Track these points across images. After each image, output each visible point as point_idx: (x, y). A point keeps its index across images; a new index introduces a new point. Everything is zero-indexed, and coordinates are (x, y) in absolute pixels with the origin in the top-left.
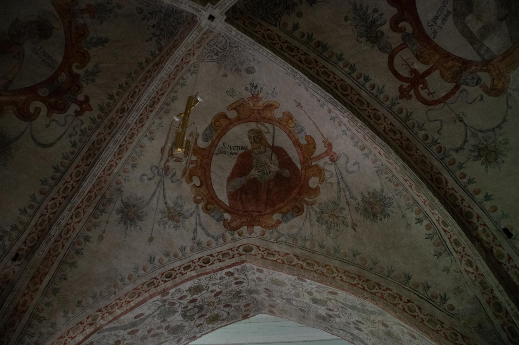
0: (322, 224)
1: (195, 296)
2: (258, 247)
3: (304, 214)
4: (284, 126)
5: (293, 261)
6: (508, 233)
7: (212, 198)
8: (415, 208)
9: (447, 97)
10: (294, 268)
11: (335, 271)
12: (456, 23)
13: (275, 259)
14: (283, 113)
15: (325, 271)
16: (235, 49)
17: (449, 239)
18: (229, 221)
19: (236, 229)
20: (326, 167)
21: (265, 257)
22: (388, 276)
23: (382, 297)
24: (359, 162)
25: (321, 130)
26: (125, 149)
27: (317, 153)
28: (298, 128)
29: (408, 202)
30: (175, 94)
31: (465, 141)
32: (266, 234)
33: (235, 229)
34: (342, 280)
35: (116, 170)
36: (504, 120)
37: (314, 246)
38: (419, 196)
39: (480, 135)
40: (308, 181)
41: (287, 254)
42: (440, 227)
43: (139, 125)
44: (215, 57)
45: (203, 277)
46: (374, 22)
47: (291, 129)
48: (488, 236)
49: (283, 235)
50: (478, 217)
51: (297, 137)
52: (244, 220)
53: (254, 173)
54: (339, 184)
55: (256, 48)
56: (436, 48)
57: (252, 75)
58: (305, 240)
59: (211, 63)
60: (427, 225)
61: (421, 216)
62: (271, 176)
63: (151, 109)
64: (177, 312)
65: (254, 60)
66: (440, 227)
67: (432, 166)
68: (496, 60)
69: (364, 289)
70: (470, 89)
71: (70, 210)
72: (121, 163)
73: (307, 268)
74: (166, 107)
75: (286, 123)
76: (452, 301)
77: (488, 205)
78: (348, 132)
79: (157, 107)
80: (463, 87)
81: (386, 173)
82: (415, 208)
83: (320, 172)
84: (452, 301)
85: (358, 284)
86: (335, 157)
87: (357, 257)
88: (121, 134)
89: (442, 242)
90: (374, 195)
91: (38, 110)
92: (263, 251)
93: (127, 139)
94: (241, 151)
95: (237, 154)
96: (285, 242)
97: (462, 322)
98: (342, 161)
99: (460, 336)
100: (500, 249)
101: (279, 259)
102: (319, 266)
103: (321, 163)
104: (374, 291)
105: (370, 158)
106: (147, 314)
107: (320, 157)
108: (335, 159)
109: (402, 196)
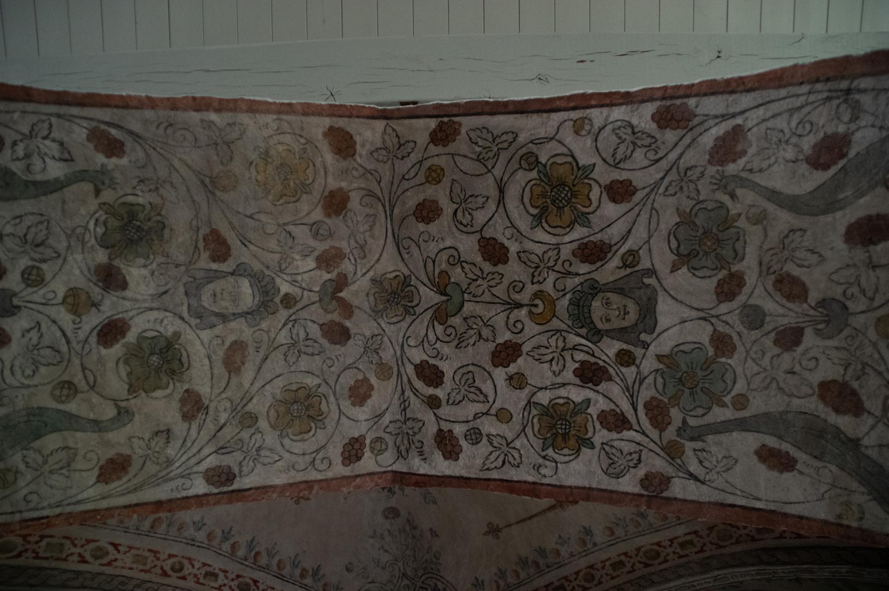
1: (577, 395)
16: (409, 573)
26: (641, 553)
30: (519, 570)
35: (680, 531)
43: (598, 575)
45: (525, 475)
57: (389, 506)
59: (448, 579)
63: (566, 584)
64: (659, 358)
65: (382, 535)
72: (663, 536)
74: (541, 562)
106: (751, 441)
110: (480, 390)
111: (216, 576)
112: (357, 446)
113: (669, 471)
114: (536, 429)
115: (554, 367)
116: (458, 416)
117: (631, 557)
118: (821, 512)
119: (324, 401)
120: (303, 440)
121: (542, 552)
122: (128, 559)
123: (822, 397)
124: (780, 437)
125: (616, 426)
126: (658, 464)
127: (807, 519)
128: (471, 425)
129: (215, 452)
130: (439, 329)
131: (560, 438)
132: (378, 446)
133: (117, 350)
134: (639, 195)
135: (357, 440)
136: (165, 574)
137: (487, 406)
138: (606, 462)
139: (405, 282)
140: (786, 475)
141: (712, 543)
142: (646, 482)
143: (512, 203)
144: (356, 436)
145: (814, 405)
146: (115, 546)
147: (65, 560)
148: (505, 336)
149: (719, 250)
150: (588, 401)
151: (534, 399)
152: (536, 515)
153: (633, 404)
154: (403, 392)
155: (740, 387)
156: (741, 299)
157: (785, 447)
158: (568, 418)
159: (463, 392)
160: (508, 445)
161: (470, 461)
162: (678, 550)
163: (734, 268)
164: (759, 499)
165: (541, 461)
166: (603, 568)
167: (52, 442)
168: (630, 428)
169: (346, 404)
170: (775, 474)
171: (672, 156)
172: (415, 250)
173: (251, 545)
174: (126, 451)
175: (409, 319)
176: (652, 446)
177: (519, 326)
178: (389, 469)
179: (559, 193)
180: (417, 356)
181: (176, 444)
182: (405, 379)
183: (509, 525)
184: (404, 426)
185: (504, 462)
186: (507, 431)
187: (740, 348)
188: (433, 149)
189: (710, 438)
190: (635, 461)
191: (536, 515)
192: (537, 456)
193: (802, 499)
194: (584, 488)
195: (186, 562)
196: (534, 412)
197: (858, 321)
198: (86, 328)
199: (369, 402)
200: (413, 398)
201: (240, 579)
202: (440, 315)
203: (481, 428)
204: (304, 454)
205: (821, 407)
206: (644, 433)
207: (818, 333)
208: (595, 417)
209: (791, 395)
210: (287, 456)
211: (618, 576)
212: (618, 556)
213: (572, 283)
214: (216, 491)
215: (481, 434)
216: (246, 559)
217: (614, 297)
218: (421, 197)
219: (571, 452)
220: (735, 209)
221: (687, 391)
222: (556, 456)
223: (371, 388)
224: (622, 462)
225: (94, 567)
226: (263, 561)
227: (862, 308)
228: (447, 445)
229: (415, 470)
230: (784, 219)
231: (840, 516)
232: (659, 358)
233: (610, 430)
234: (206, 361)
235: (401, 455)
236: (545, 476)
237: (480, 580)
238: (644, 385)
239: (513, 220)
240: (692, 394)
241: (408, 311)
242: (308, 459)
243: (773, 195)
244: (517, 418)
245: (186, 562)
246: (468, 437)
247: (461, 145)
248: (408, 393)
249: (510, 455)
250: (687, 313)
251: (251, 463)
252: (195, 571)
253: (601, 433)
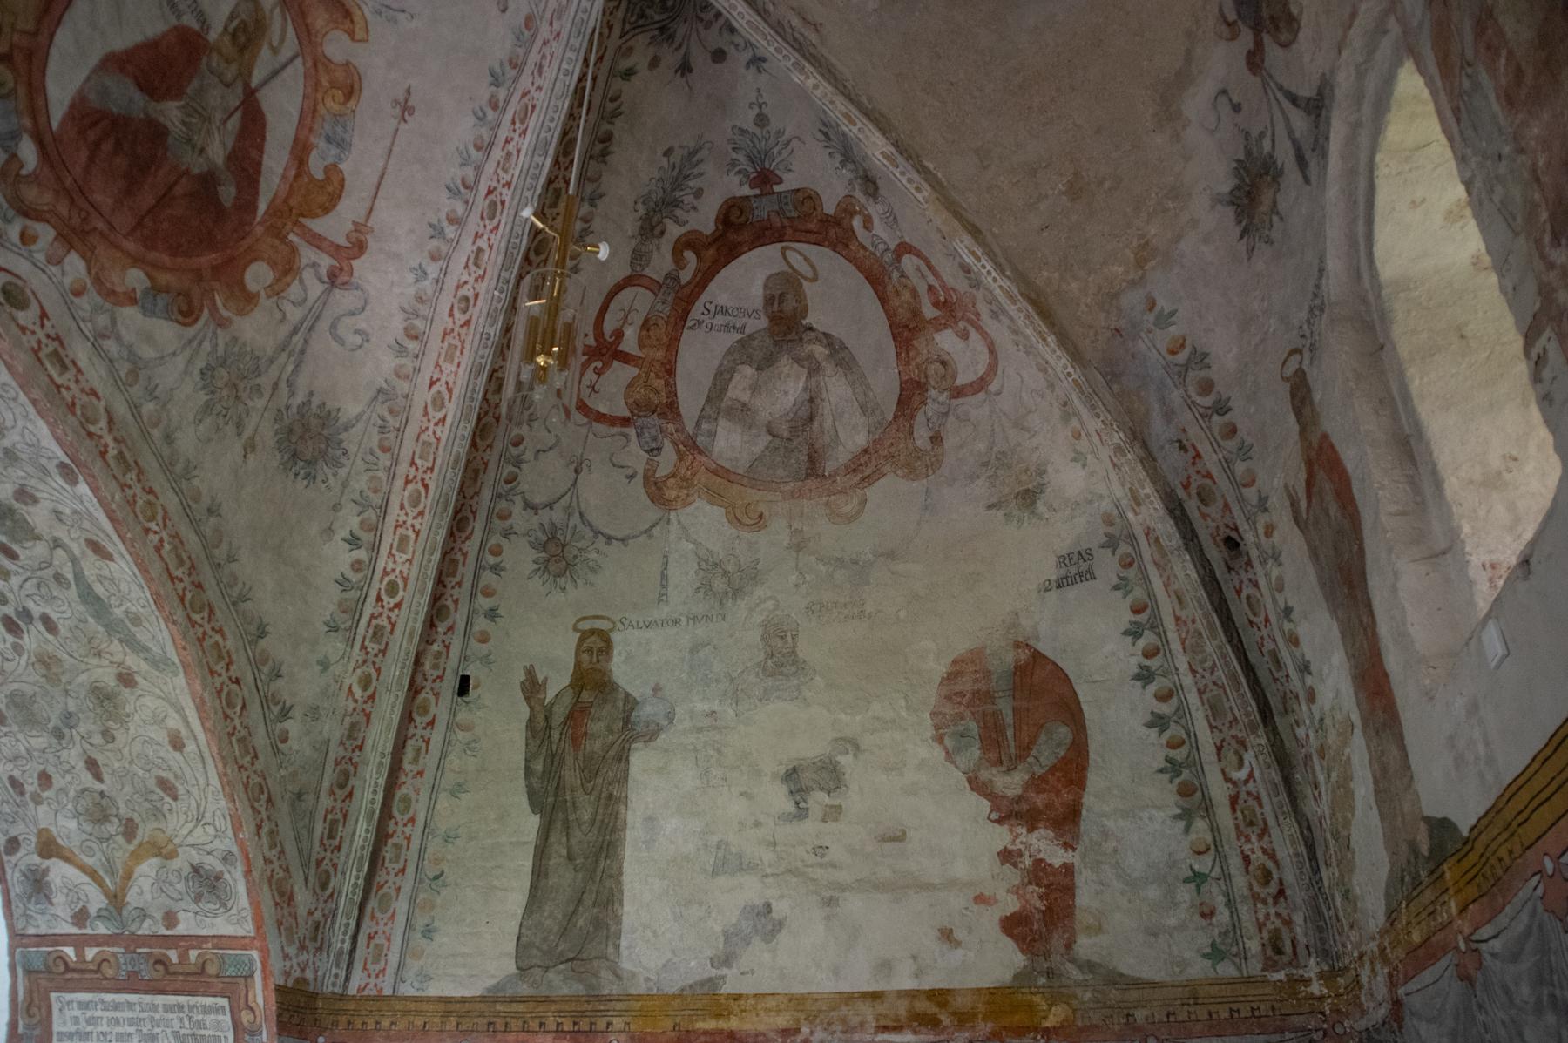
0: (204, 388)
2: (44, 315)
3: (191, 331)
4: (317, 84)
5: (94, 422)
6: (464, 686)
7: (30, 55)
8: (371, 515)
9: (601, 418)
10: (88, 441)
11: (159, 518)
12: (729, 352)
13: (59, 380)
14: (348, 64)
15: (140, 502)
17: (372, 617)
18: (24, 172)
19: (26, 214)
20: (308, 275)
21: (42, 355)
22: (234, 604)
23: (201, 640)
24: (373, 339)
25: (380, 203)
27: (318, 225)
28: (339, 129)
29: (372, 495)
31: (549, 506)
32: (85, 298)
33: (26, 212)
34: (158, 549)
36: (622, 540)
37: (156, 425)
38: (402, 507)
39: (575, 520)
40: (251, 262)
41: (94, 393)
42: (378, 585)
46: (676, 203)
47: (322, 110)
48: (436, 666)
49: (119, 339)
50: (451, 629)
51: (313, 139)
52: (63, 209)
53: (171, 113)
54: (295, 331)
55: (572, 41)
56: (673, 343)
58: (151, 393)
60: (359, 562)
61: (366, 537)
62: (198, 166)
66: (378, 585)
67: (477, 493)
68: (704, 459)
69: (182, 599)
70: (634, 445)
73: (112, 463)
75: (325, 84)
76: (293, 726)
77: (481, 624)
78: (427, 283)
80: (632, 432)
81: (391, 411)
82: (371, 515)
83: (287, 269)
84: (293, 726)
85: (181, 580)
86: (343, 278)
87: (212, 520)
89: (355, 611)
90: (327, 417)
92: (48, 336)
94: (189, 20)
95: (179, 17)
96: (111, 361)
97: (283, 772)
98: (344, 299)
99: (264, 797)
100: (433, 699)
101: (68, 388)
102: (139, 481)
103: (307, 254)
104: (196, 617)
105: (403, 361)
107: (317, 241)
108: (339, 281)
109: (371, 473)
111: (480, 250)
122: (449, 368)
133: (16, 548)
136: (467, 323)
146: (432, 383)
147: (438, 440)
167: (99, 589)
173: (453, 192)
174: (82, 541)
181: (60, 508)
195: (462, 292)
198: (14, 567)
210: (20, 423)
216: (467, 202)
225: (452, 409)
242: (12, 404)
245: (462, 292)
252: (472, 280)
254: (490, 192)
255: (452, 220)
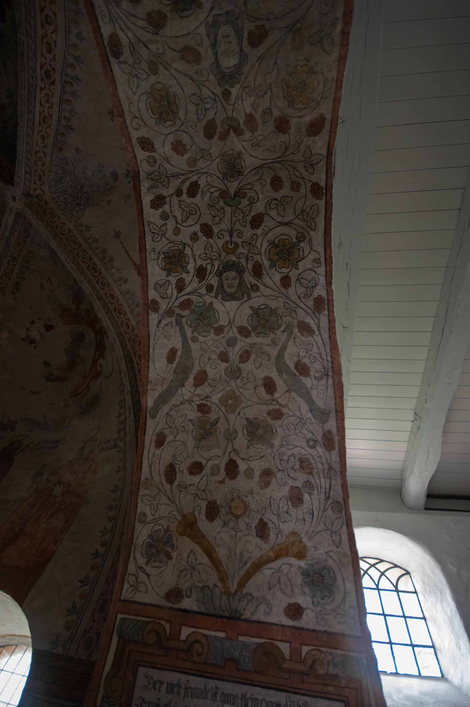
1: (191, 267)
26: (120, 307)
44: (82, 207)
45: (149, 244)
63: (98, 273)
64: (211, 303)
71: (125, 377)
79: (100, 265)
88: (94, 303)
91: (101, 366)
93: (112, 301)
106: (178, 345)
110: (188, 218)
112: (149, 147)
113: (161, 312)
114: (172, 248)
115: (203, 256)
116: (173, 206)
117: (117, 302)
118: (152, 375)
119: (172, 123)
120: (147, 110)
121: (111, 260)
123: (200, 372)
124: (181, 356)
125: (178, 286)
126: (163, 306)
127: (148, 370)
128: (170, 214)
129: (130, 42)
130: (217, 194)
131: (169, 260)
132: (151, 161)
134: (284, 291)
135: (153, 147)
137: (180, 222)
138: (161, 283)
139: (240, 173)
140: (165, 361)
141: (130, 337)
142: (155, 302)
143: (280, 230)
144: (155, 146)
145: (196, 369)
148: (216, 229)
149: (260, 326)
150: (188, 272)
151: (186, 246)
152: (129, 256)
153: (189, 293)
154: (182, 175)
155: (201, 339)
156: (239, 337)
157: (178, 359)
158: (179, 263)
159: (186, 209)
160: (163, 234)
161: (152, 215)
162: (124, 323)
163: (252, 333)
164: (154, 350)
165: (157, 252)
166: (110, 290)
168: (178, 293)
169: (171, 138)
170: (166, 356)
171: (302, 305)
172: (256, 177)
175: (221, 176)
176: (171, 303)
177: (221, 237)
178: (140, 169)
179: (285, 253)
180: (202, 182)
182: (189, 175)
183: (121, 243)
184: (164, 176)
185: (154, 233)
186: (169, 234)
187: (218, 338)
188: (309, 185)
189: (178, 328)
190: (163, 296)
191: (129, 256)
192: (160, 249)
193: (156, 367)
194: (147, 274)
196: (180, 247)
197: (233, 383)
199: (174, 154)
200: (180, 180)
201: (52, 71)
202: (224, 194)
203: (169, 220)
204: (139, 110)
205: (196, 371)
206: (176, 299)
207: (227, 368)
208: (181, 276)
209: (200, 360)
211: (107, 297)
212: (117, 297)
213: (243, 261)
214: (106, 42)
215: (166, 220)
216: (66, 75)
217: (237, 281)
218: (284, 180)
219: (163, 266)
220: (278, 332)
221: (197, 317)
222: (160, 259)
223: (183, 155)
224: (162, 290)
226: (68, 89)
227: (238, 384)
228: (158, 202)
229: (142, 184)
230: (274, 352)
231: (151, 382)
232: (211, 303)
233: (176, 284)
234: (186, 32)
235: (149, 175)
236: (150, 254)
237: (90, 229)
238: (198, 298)
239: (271, 231)
240: (196, 319)
241: (225, 175)
242: (137, 114)
243: (284, 348)
244: (176, 238)
246: (164, 213)
247: (311, 200)
248: (182, 178)
249: (157, 236)
250: (232, 314)
251: (127, 71)
253: (174, 280)
254: (53, 83)
255: (71, 65)
